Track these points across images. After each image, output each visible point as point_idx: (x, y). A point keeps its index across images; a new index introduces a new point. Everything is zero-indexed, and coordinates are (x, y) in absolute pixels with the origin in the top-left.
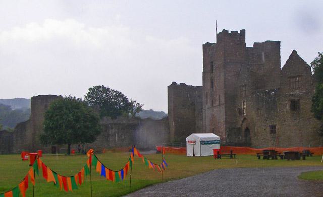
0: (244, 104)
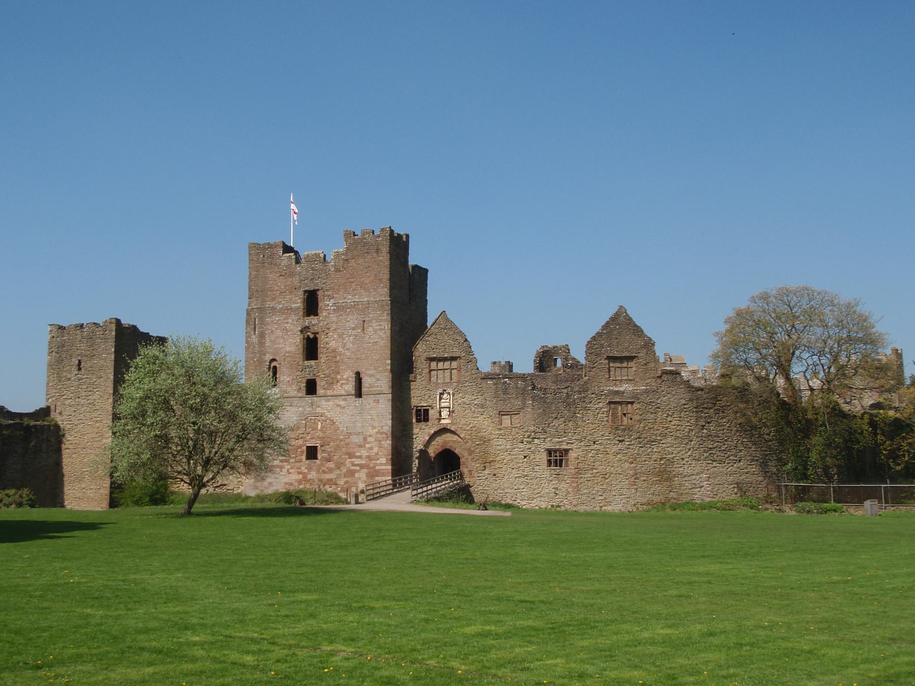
0: (441, 399)
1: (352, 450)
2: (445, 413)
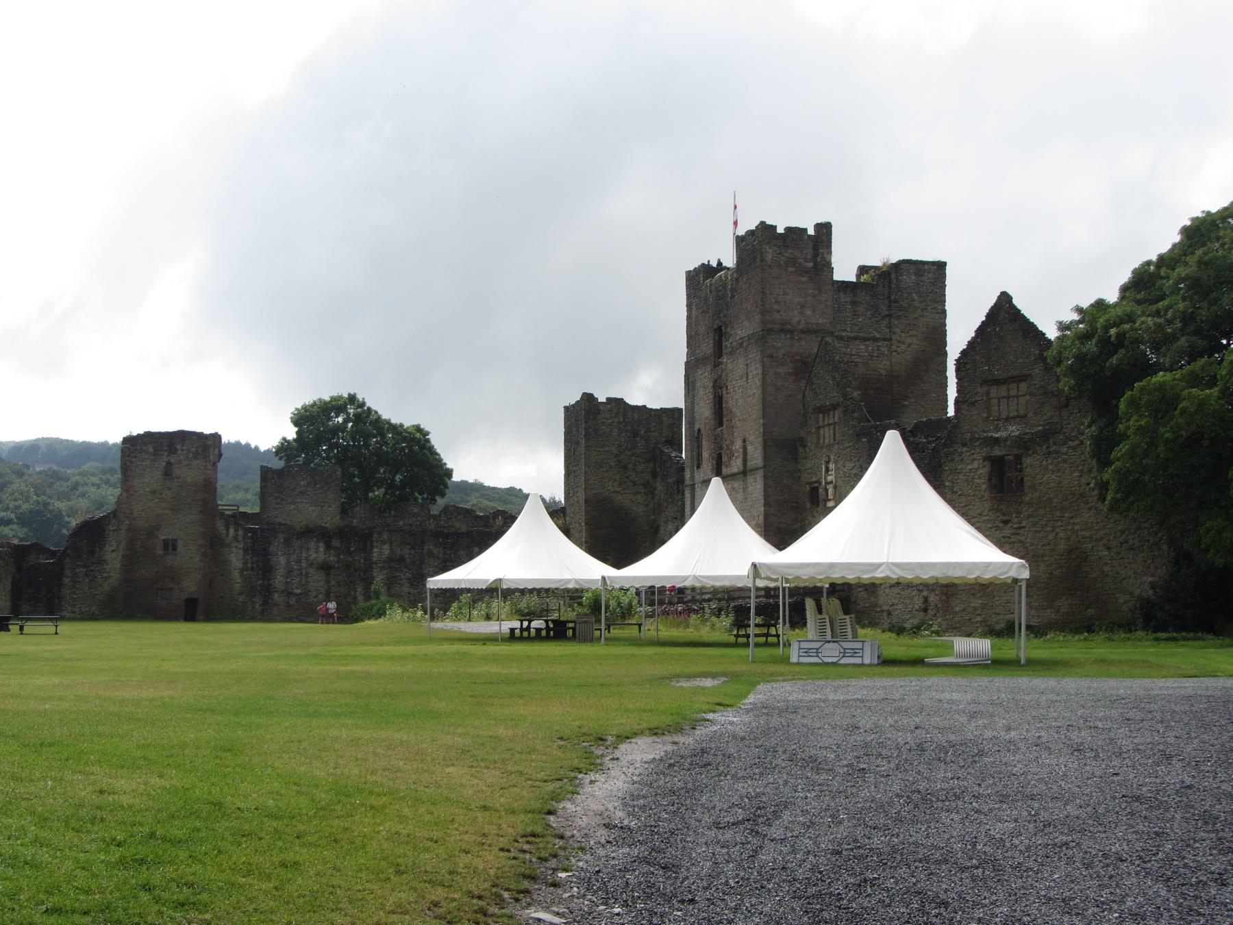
0: (827, 470)
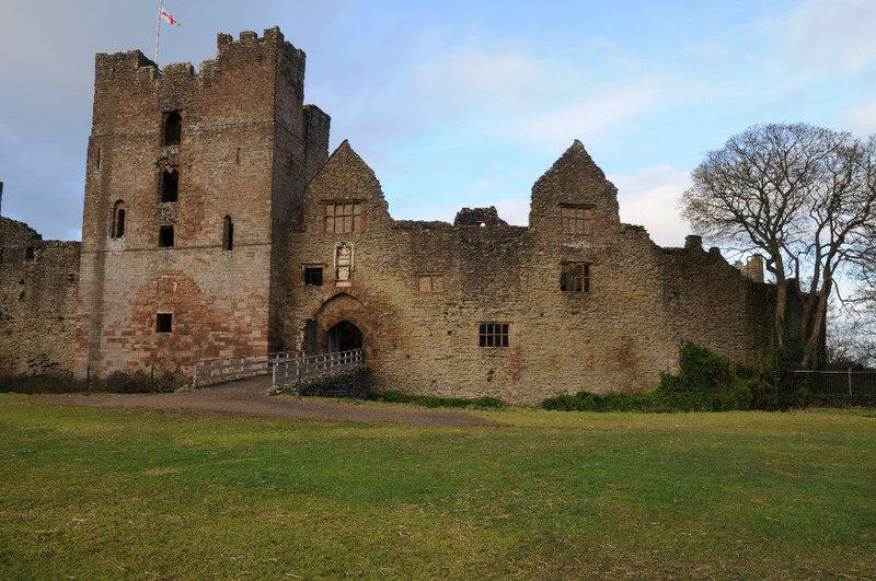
0: (338, 254)
1: (217, 320)
2: (343, 274)
